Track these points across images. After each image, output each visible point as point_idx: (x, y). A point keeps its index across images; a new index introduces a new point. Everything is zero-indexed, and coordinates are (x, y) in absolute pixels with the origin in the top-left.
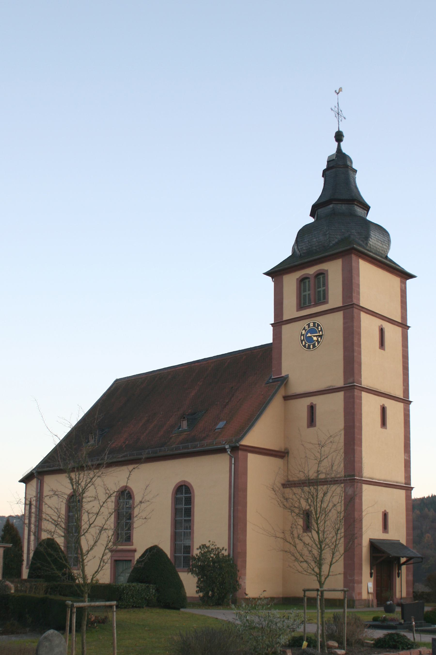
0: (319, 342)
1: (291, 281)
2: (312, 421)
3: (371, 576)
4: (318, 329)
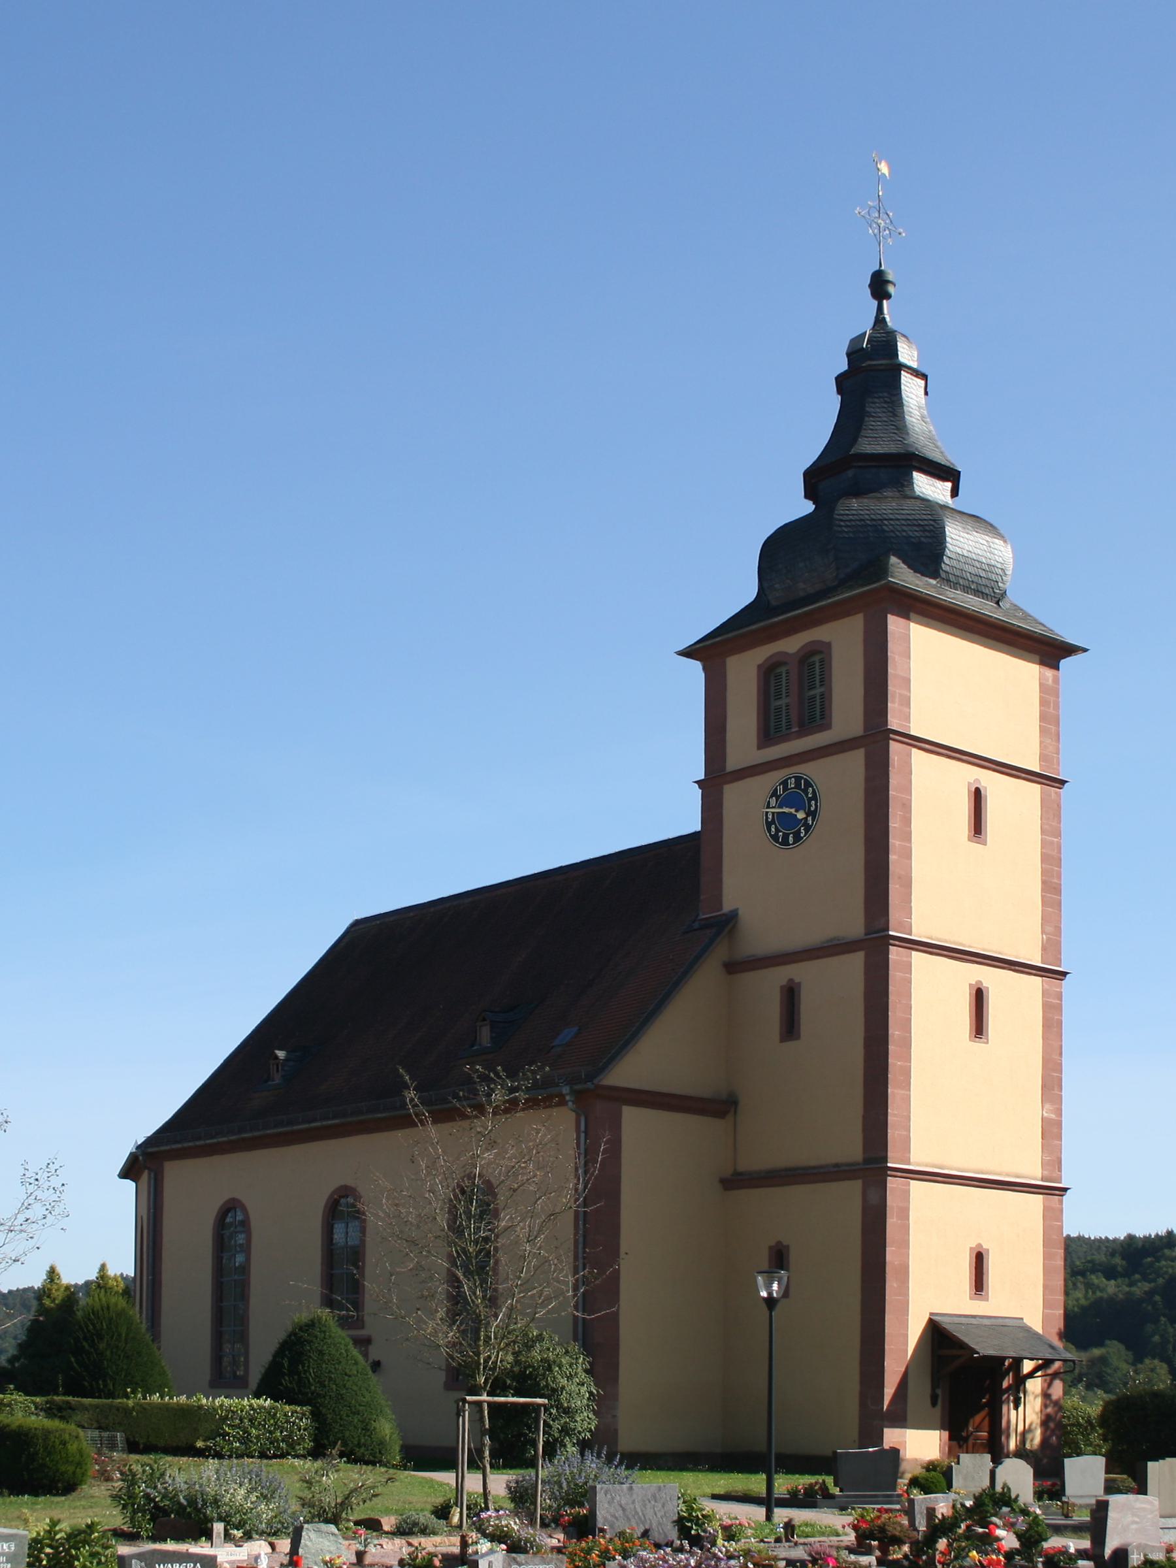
0: (808, 828)
1: (744, 670)
2: (790, 1027)
3: (934, 1404)
4: (807, 794)
